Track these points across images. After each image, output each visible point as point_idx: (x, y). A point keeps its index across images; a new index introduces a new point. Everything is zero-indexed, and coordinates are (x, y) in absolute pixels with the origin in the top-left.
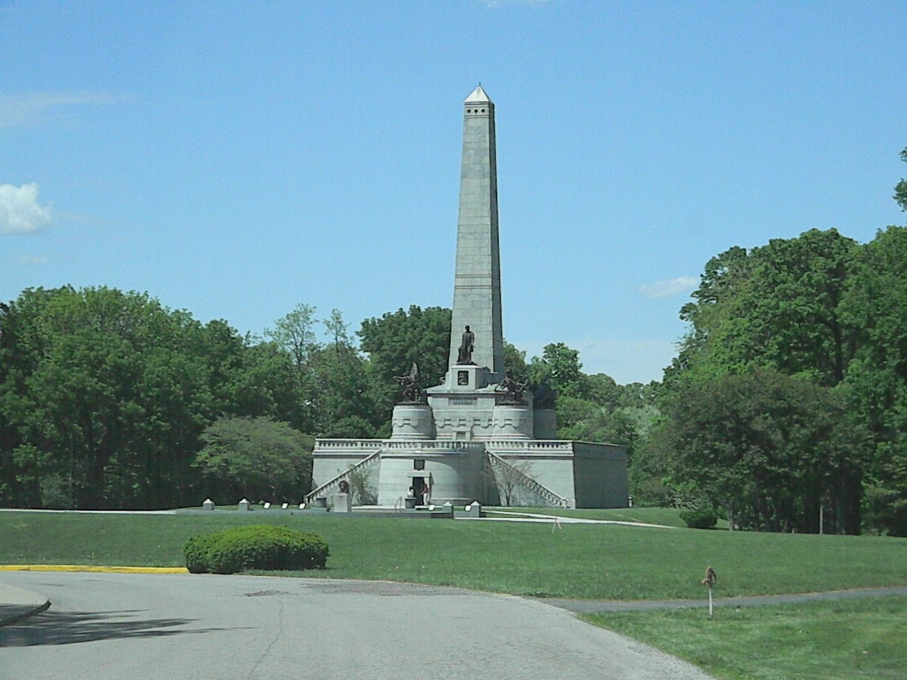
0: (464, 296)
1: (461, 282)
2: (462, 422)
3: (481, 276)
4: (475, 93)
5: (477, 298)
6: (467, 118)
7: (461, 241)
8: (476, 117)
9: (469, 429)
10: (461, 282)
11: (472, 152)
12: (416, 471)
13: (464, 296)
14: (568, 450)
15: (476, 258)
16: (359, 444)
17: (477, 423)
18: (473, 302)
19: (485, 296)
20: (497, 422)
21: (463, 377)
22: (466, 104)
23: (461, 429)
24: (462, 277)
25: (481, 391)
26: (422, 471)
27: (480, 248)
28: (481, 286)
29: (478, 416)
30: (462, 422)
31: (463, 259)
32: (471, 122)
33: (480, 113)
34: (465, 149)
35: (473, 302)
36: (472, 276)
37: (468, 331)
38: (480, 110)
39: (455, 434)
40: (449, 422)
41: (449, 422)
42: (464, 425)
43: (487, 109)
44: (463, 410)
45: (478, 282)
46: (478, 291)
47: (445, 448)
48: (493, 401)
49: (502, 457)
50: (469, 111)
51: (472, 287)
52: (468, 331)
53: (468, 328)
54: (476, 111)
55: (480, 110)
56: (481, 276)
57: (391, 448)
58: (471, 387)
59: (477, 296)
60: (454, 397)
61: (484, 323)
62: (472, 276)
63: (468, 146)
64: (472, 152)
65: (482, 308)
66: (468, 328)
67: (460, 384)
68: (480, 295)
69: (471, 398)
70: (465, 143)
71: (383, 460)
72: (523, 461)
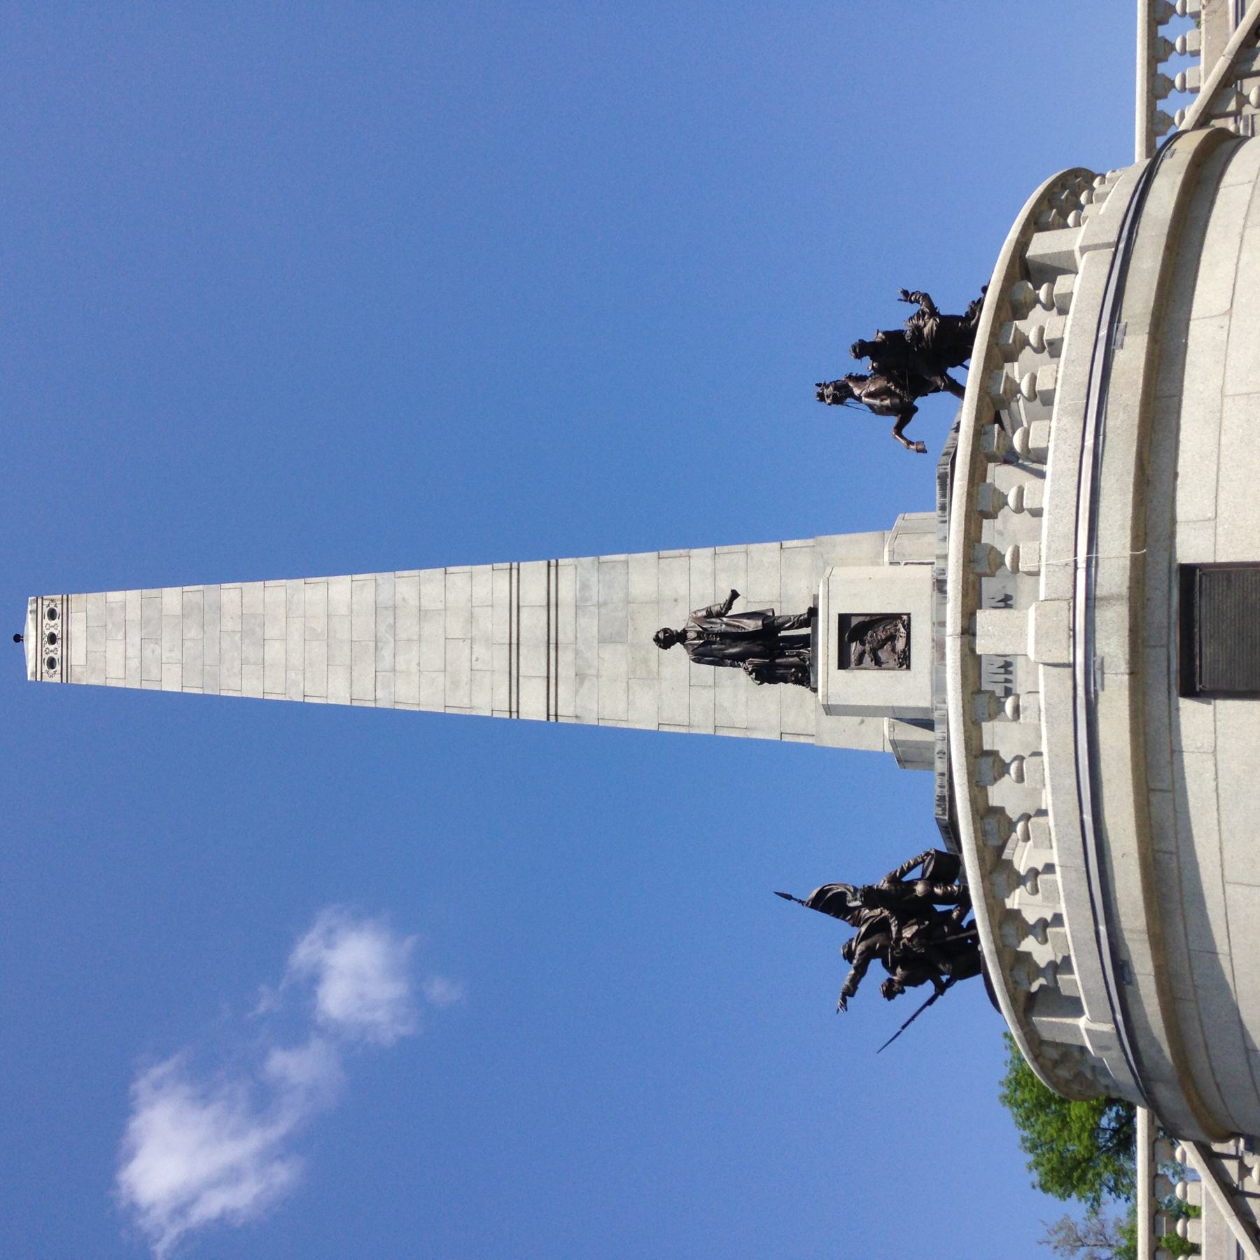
3: (515, 608)
5: (590, 625)
11: (149, 647)
13: (580, 677)
15: (456, 627)
18: (602, 640)
27: (422, 614)
28: (551, 605)
31: (456, 684)
33: (54, 627)
35: (602, 640)
36: (514, 646)
37: (681, 637)
45: (534, 623)
46: (566, 615)
51: (552, 644)
53: (667, 639)
54: (52, 639)
56: (515, 608)
59: (583, 621)
61: (683, 590)
62: (514, 646)
63: (134, 664)
65: (628, 601)
66: (667, 639)
67: (904, 661)
68: (578, 607)
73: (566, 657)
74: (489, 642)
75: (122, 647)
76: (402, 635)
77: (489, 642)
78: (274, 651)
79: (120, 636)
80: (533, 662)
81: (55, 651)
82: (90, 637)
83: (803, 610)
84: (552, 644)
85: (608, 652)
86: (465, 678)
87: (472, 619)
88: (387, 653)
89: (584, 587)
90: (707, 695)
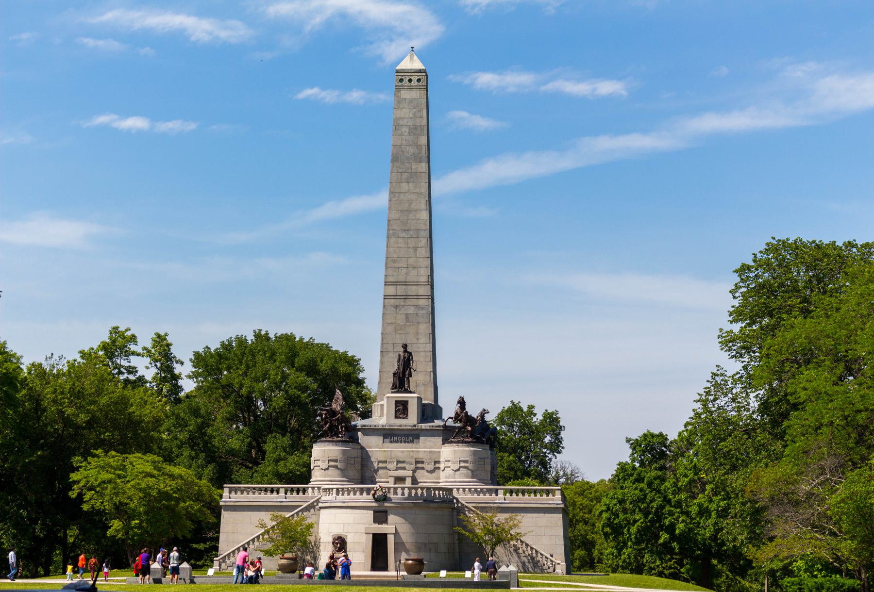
0: (396, 307)
1: (391, 290)
2: (400, 465)
3: (417, 284)
4: (408, 57)
5: (411, 310)
6: (398, 89)
7: (393, 240)
8: (411, 88)
9: (410, 473)
10: (391, 290)
12: (376, 526)
13: (396, 307)
14: (556, 499)
15: (411, 261)
16: (282, 491)
17: (420, 465)
18: (407, 315)
19: (423, 308)
20: (447, 464)
21: (401, 409)
22: (397, 72)
23: (400, 473)
24: (395, 284)
25: (424, 426)
26: (384, 526)
27: (415, 249)
28: (418, 297)
29: (421, 456)
30: (400, 465)
31: (394, 261)
32: (405, 95)
34: (397, 126)
35: (407, 315)
38: (415, 79)
39: (392, 480)
40: (384, 465)
41: (384, 465)
42: (404, 468)
43: (423, 78)
44: (400, 450)
45: (412, 290)
46: (414, 302)
47: (399, 496)
48: (439, 440)
49: (475, 507)
50: (401, 80)
51: (406, 297)
52: (405, 351)
53: (405, 346)
54: (410, 81)
55: (415, 79)
56: (417, 284)
57: (340, 497)
58: (412, 419)
60: (389, 434)
61: (421, 341)
62: (406, 284)
63: (401, 123)
64: (404, 129)
65: (418, 323)
66: (405, 346)
67: (396, 417)
69: (411, 436)
70: (397, 119)
71: (322, 511)
72: (507, 515)
73: (402, 302)
74: (407, 274)
75: (407, 116)
76: (409, 240)
77: (407, 274)
78: (405, 187)
79: (411, 116)
80: (400, 290)
81: (406, 82)
82: (411, 101)
83: (412, 389)
84: (406, 297)
85: (403, 317)
86: (396, 265)
87: (414, 268)
88: (404, 235)
89: (423, 308)
90: (391, 349)
